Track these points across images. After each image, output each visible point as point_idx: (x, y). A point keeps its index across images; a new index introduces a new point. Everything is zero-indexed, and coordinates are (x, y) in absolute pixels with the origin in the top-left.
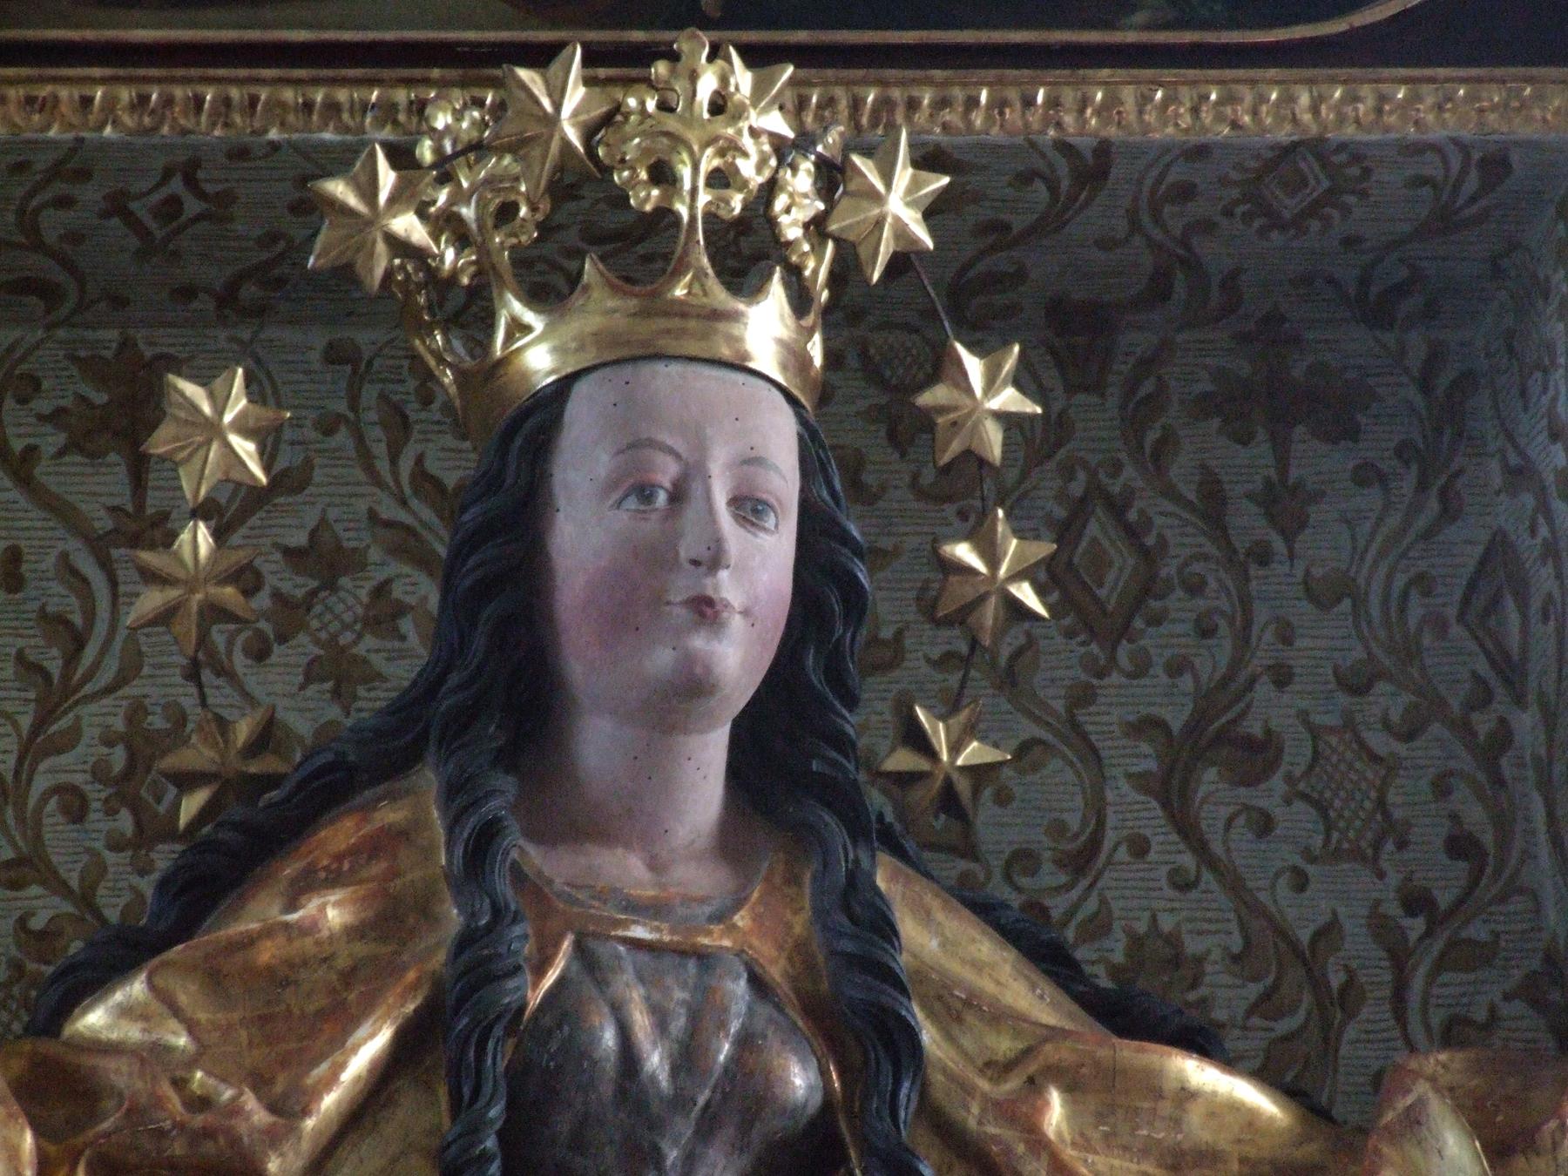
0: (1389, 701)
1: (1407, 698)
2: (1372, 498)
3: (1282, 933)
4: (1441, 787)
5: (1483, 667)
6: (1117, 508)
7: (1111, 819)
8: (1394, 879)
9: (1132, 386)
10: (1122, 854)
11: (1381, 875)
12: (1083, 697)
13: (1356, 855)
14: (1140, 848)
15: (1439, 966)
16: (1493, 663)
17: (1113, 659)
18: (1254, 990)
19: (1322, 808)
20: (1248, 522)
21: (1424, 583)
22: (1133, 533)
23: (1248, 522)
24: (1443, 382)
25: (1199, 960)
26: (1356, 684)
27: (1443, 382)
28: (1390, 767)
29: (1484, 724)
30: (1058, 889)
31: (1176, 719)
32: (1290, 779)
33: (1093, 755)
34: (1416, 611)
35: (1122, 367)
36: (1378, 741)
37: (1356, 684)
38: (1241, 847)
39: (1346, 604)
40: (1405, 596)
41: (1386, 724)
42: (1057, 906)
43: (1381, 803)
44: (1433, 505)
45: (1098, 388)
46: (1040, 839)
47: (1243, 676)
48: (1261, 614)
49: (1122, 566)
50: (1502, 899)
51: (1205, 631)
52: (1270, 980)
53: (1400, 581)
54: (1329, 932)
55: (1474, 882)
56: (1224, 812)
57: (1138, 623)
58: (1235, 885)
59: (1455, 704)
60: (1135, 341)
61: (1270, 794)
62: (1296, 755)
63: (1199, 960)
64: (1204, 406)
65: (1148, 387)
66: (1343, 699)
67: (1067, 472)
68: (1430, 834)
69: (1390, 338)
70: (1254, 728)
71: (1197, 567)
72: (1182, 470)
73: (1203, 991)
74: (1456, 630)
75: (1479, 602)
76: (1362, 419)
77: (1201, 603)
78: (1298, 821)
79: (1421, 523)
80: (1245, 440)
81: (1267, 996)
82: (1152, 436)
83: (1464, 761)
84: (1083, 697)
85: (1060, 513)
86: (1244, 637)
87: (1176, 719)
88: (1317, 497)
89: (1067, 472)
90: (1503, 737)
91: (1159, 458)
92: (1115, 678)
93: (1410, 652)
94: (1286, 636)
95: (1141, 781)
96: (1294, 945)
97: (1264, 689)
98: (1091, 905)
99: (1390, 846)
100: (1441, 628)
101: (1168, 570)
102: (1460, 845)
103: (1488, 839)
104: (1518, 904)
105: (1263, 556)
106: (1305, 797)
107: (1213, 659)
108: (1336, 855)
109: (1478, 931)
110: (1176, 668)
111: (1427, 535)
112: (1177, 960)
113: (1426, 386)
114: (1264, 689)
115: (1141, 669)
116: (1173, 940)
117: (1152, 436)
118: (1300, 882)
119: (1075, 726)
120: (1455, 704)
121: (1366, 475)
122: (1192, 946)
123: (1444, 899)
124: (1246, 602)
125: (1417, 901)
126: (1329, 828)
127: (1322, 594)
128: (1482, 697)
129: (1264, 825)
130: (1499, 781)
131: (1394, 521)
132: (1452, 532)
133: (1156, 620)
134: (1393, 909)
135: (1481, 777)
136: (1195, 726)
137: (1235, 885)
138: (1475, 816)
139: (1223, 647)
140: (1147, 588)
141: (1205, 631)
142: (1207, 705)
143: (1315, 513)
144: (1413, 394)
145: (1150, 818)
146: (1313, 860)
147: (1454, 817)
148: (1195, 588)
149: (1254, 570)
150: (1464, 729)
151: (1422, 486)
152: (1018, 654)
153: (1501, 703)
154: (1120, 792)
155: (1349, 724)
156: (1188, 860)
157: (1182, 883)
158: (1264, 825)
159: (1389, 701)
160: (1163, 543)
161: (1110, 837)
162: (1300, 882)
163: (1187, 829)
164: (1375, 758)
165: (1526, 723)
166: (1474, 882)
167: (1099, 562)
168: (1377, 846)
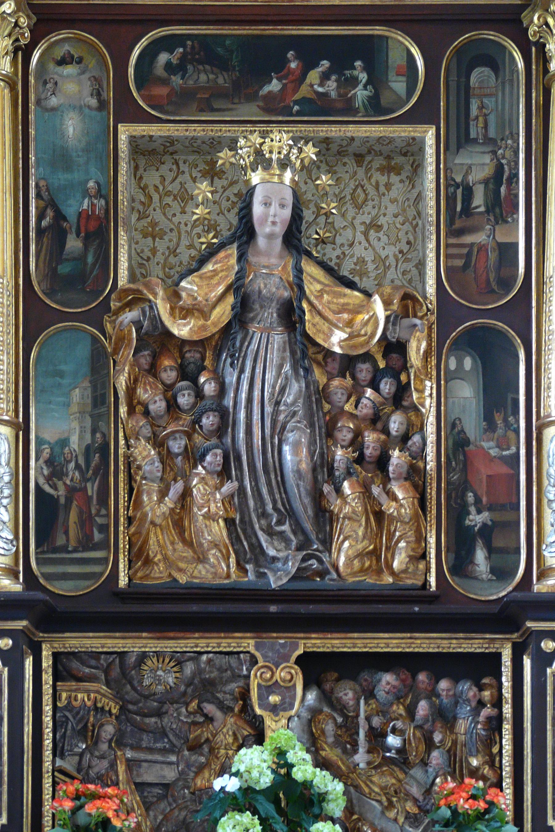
0: (400, 219)
4: (407, 233)
5: (415, 213)
6: (362, 187)
13: (393, 244)
14: (360, 243)
15: (403, 262)
20: (382, 189)
22: (364, 191)
23: (382, 189)
28: (399, 230)
29: (414, 223)
36: (398, 226)
37: (396, 216)
38: (375, 243)
43: (397, 236)
48: (383, 204)
51: (374, 208)
54: (387, 257)
58: (374, 249)
62: (385, 228)
68: (404, 241)
70: (379, 223)
74: (412, 207)
75: (416, 203)
77: (374, 203)
78: (384, 239)
79: (409, 189)
83: (411, 229)
84: (354, 218)
87: (368, 223)
88: (393, 185)
93: (404, 211)
94: (386, 209)
95: (361, 232)
97: (382, 217)
100: (410, 207)
101: (369, 197)
103: (413, 242)
105: (384, 195)
107: (374, 212)
108: (390, 244)
110: (369, 214)
111: (410, 191)
112: (363, 262)
114: (382, 217)
118: (384, 249)
119: (352, 223)
123: (405, 251)
130: (415, 232)
131: (405, 189)
134: (397, 253)
138: (411, 238)
139: (376, 210)
140: (366, 200)
141: (374, 208)
148: (373, 200)
154: (358, 234)
155: (394, 223)
156: (367, 245)
158: (379, 239)
159: (400, 219)
162: (384, 249)
163: (367, 240)
165: (420, 223)
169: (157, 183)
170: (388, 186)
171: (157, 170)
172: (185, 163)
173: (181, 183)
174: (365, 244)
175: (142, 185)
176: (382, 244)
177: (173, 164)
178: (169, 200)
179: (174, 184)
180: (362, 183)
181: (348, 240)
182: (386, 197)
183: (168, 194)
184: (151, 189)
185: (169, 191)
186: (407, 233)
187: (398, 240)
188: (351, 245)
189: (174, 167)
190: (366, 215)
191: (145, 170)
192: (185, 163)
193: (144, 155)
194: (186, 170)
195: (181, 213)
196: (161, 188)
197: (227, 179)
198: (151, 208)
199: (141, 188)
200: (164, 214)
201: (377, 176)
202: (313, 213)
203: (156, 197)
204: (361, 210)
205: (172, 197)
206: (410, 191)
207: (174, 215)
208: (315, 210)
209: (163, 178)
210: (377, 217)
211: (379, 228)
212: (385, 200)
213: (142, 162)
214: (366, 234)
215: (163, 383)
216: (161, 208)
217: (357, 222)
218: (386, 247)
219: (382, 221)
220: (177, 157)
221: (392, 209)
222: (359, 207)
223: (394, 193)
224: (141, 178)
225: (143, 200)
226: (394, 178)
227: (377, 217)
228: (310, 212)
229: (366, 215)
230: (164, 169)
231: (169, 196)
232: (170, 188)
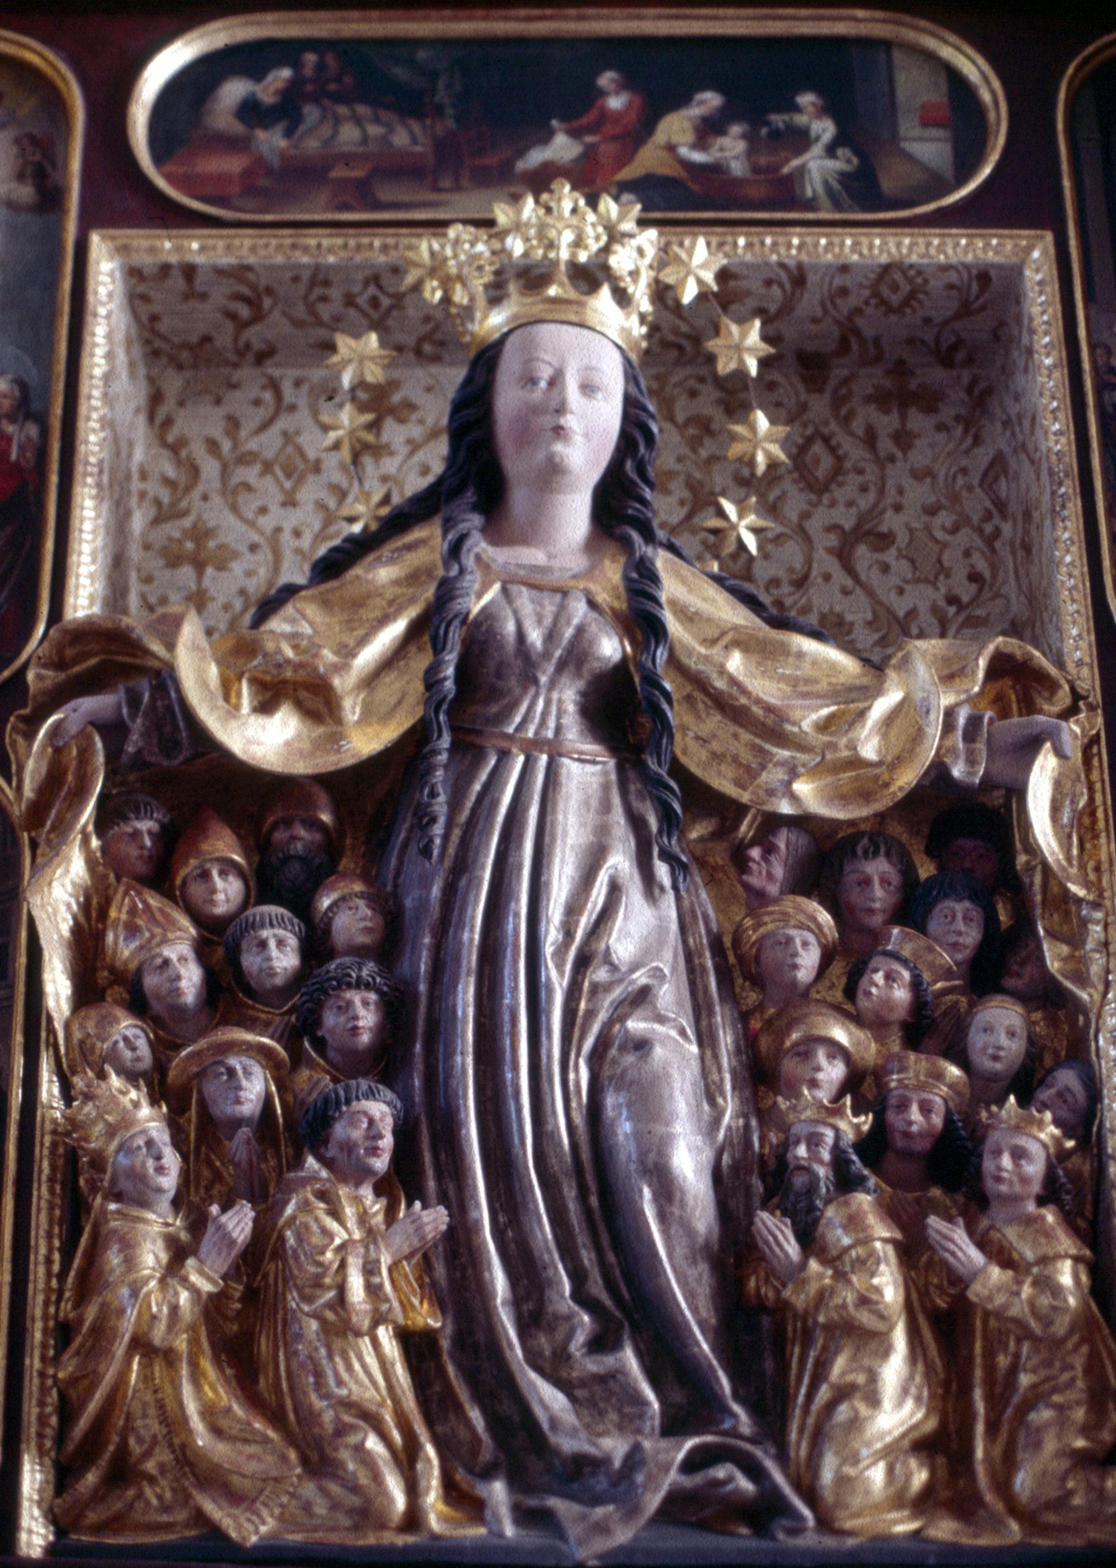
0: (945, 518)
1: (954, 517)
2: (941, 437)
3: (890, 612)
4: (967, 554)
5: (988, 504)
6: (826, 440)
7: (815, 565)
8: (943, 590)
9: (836, 391)
10: (820, 580)
11: (937, 589)
12: (805, 516)
13: (926, 581)
14: (827, 578)
16: (993, 503)
17: (820, 501)
18: (876, 636)
19: (913, 562)
20: (886, 445)
21: (964, 471)
22: (833, 450)
23: (886, 445)
24: (976, 391)
25: (852, 624)
26: (931, 511)
27: (976, 391)
28: (944, 546)
29: (988, 528)
30: (790, 595)
31: (848, 525)
32: (899, 550)
33: (807, 539)
34: (960, 481)
35: (831, 384)
36: (939, 534)
37: (931, 511)
38: (873, 577)
39: (928, 480)
40: (954, 478)
41: (944, 528)
42: (788, 601)
43: (939, 561)
44: (969, 441)
45: (820, 391)
46: (782, 574)
47: (881, 506)
48: (890, 483)
49: (826, 463)
50: (992, 599)
51: (864, 489)
52: (884, 631)
53: (953, 470)
55: (980, 591)
56: (866, 564)
57: (833, 486)
58: (870, 593)
59: (975, 519)
60: (839, 372)
61: (890, 556)
62: (902, 539)
63: (852, 624)
64: (869, 399)
65: (844, 391)
66: (925, 518)
67: (805, 425)
69: (955, 373)
70: (884, 528)
71: (862, 464)
72: (858, 426)
73: (853, 636)
74: (978, 490)
75: (990, 478)
76: (940, 405)
78: (901, 568)
79: (965, 446)
80: (887, 412)
81: (883, 638)
82: (844, 411)
83: (979, 543)
84: (805, 516)
85: (800, 441)
86: (881, 491)
87: (848, 525)
88: (919, 436)
89: (805, 425)
90: (997, 533)
91: (846, 421)
92: (820, 509)
93: (955, 498)
94: (901, 491)
95: (830, 551)
96: (896, 618)
97: (889, 514)
98: (804, 600)
99: (942, 577)
100: (970, 489)
101: (848, 464)
102: (974, 577)
103: (987, 575)
104: (999, 602)
105: (892, 459)
106: (906, 557)
107: (865, 502)
108: (917, 581)
109: (980, 612)
110: (850, 504)
111: (967, 452)
113: (969, 390)
114: (889, 514)
115: (833, 504)
116: (840, 616)
117: (844, 411)
118: (901, 591)
120: (975, 519)
121: (941, 427)
122: (849, 617)
123: (965, 598)
124: (883, 478)
125: (952, 600)
126: (915, 568)
127: (918, 475)
128: (988, 517)
129: (885, 568)
130: (993, 550)
131: (951, 446)
132: (979, 451)
133: (840, 485)
134: (942, 603)
135: (985, 549)
136: (857, 527)
137: (870, 593)
138: (982, 566)
139: (872, 496)
140: (837, 471)
141: (864, 489)
142: (862, 519)
143: (918, 442)
144: (962, 395)
145: (833, 566)
146: (906, 582)
147: (972, 566)
148: (860, 472)
149: (889, 466)
150: (980, 531)
151: (966, 431)
152: (779, 498)
153: (997, 520)
154: (820, 554)
155: (928, 528)
156: (849, 583)
157: (845, 592)
158: (885, 568)
159: (945, 518)
160: (846, 455)
161: (814, 573)
162: (901, 591)
164: (937, 542)
165: (1007, 528)
166: (980, 591)
167: (817, 461)
168: (936, 577)
169: (217, 430)
170: (904, 439)
171: (218, 401)
172: (298, 383)
173: (285, 434)
174: (840, 578)
175: (170, 439)
176: (895, 580)
177: (264, 388)
178: (250, 474)
179: (264, 437)
180: (826, 431)
181: (791, 570)
182: (899, 464)
183: (245, 459)
184: (197, 450)
185: (250, 453)
186: (967, 554)
187: (943, 571)
188: (801, 582)
189: (268, 396)
190: (841, 508)
191: (181, 404)
192: (298, 383)
193: (180, 367)
194: (303, 402)
195: (284, 504)
196: (226, 446)
197: (421, 422)
198: (196, 494)
199: (164, 444)
200: (234, 509)
201: (866, 415)
202: (682, 503)
203: (210, 468)
204: (825, 499)
205: (257, 468)
206: (967, 452)
207: (263, 510)
208: (686, 494)
209: (233, 424)
210: (875, 512)
211: (884, 540)
212: (897, 473)
213: (173, 383)
214: (844, 555)
215: (199, 918)
216: (223, 492)
217: (814, 525)
218: (907, 587)
219: (891, 522)
220: (276, 372)
221: (918, 494)
222: (818, 488)
223: (920, 456)
224: (168, 422)
225: (171, 472)
226: (917, 420)
227: (875, 512)
228: (673, 500)
229: (841, 508)
230: (237, 402)
231: (248, 464)
232: (252, 445)
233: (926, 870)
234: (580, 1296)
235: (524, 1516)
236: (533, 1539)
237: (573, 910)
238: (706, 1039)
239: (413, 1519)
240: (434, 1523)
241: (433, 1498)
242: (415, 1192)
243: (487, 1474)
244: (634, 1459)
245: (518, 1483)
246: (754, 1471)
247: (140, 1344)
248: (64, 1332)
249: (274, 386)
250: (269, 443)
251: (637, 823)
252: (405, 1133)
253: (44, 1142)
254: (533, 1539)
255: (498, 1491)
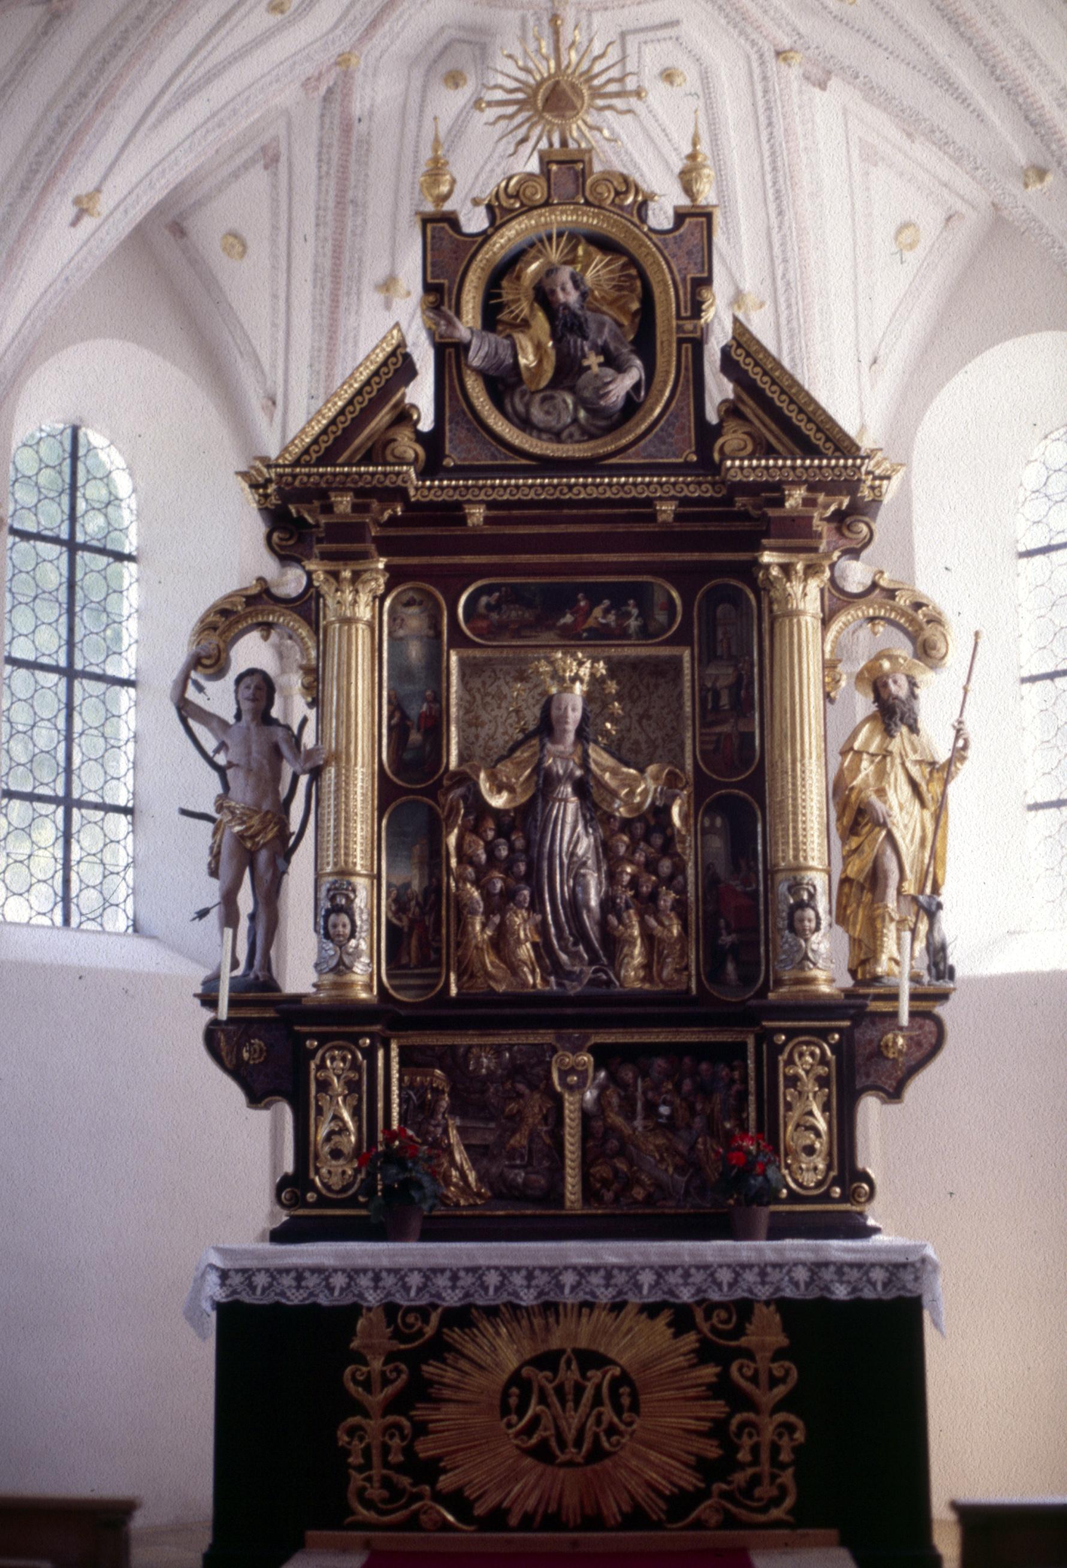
183: (487, 694)
209: (484, 683)
233: (652, 823)
234: (571, 934)
235: (559, 984)
236: (560, 990)
237: (569, 843)
238: (599, 870)
239: (534, 985)
240: (539, 987)
241: (538, 981)
242: (535, 911)
243: (550, 974)
244: (581, 972)
245: (557, 976)
246: (606, 974)
247: (477, 947)
248: (458, 945)
249: (494, 671)
250: (492, 690)
251: (584, 816)
252: (532, 896)
253: (452, 899)
254: (560, 990)
255: (552, 979)
